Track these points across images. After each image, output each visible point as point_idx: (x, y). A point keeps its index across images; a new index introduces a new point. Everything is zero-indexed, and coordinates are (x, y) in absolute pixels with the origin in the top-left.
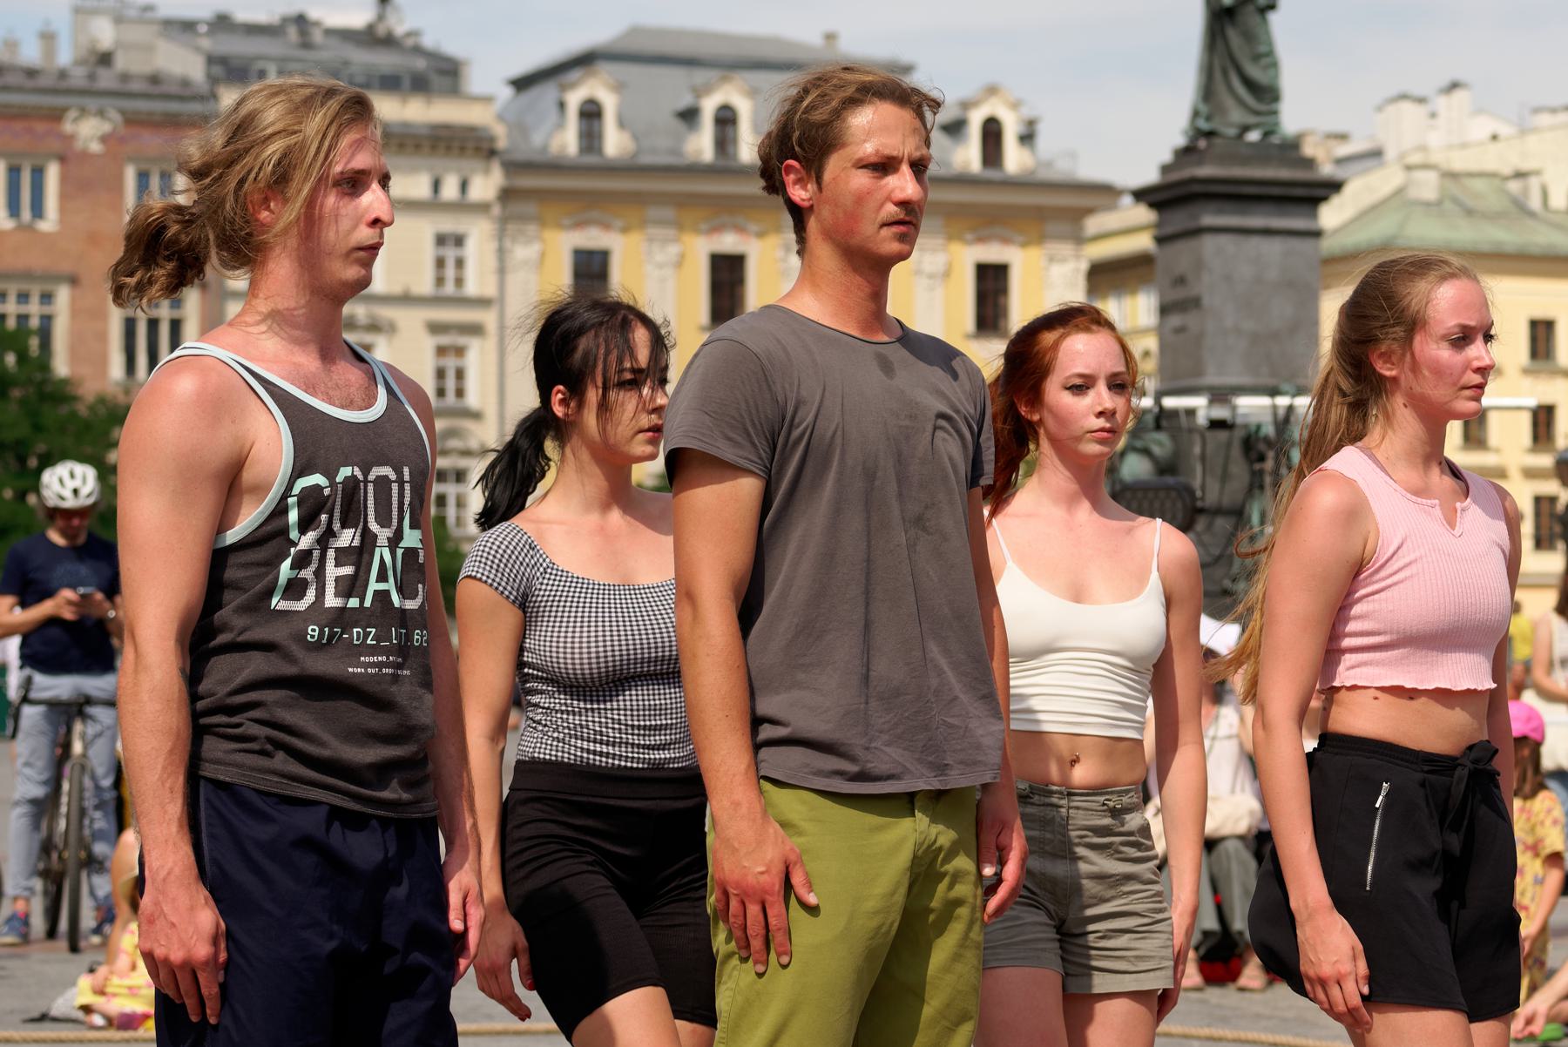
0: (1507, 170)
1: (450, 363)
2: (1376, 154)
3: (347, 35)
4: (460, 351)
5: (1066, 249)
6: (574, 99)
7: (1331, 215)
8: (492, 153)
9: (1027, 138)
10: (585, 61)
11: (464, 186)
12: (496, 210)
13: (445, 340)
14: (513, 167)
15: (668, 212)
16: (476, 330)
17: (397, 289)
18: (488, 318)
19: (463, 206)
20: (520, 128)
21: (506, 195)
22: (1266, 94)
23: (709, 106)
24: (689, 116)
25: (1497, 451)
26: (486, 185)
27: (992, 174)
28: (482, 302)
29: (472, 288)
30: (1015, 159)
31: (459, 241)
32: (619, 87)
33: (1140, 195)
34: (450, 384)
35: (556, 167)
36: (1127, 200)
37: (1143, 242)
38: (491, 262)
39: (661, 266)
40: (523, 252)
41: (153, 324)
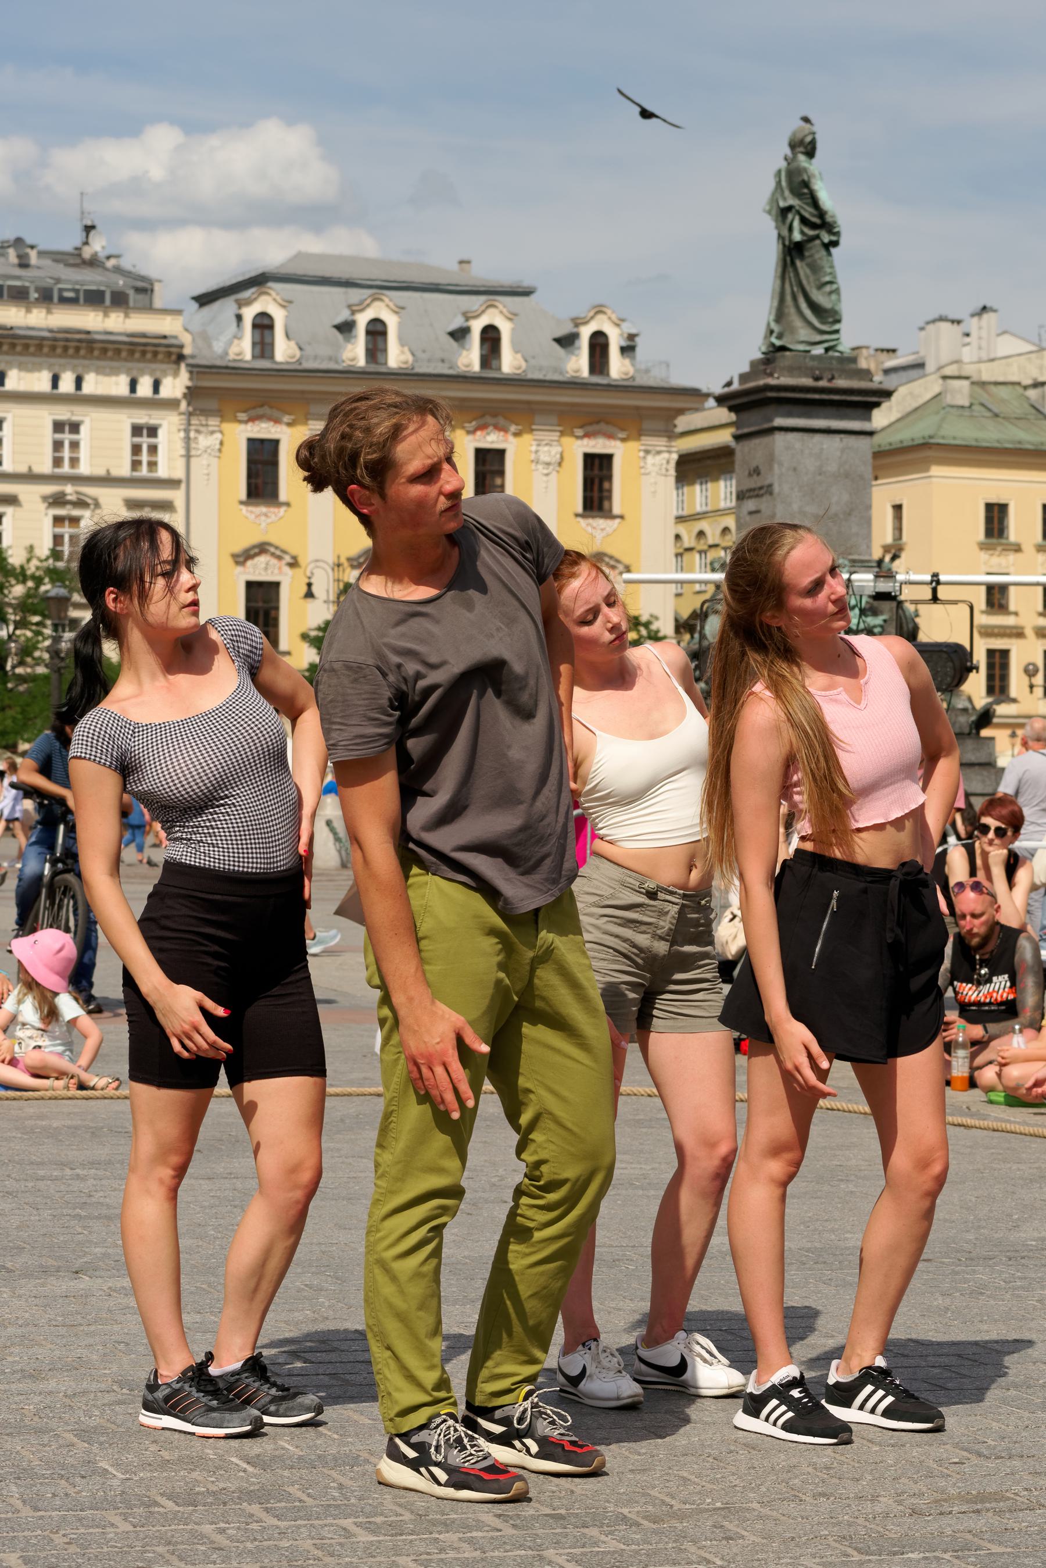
0: (1028, 382)
2: (921, 365)
3: (58, 257)
5: (660, 442)
6: (249, 313)
7: (880, 418)
8: (181, 357)
9: (627, 350)
10: (259, 281)
11: (156, 386)
12: (184, 405)
14: (198, 370)
17: (101, 472)
18: (177, 496)
19: (155, 403)
20: (203, 337)
21: (191, 393)
22: (828, 316)
23: (362, 320)
24: (346, 328)
25: (1016, 614)
26: (174, 386)
27: (597, 379)
28: (172, 483)
29: (162, 472)
30: (618, 367)
31: (153, 431)
32: (286, 304)
33: (721, 400)
35: (234, 370)
36: (711, 402)
37: (724, 437)
40: (205, 441)
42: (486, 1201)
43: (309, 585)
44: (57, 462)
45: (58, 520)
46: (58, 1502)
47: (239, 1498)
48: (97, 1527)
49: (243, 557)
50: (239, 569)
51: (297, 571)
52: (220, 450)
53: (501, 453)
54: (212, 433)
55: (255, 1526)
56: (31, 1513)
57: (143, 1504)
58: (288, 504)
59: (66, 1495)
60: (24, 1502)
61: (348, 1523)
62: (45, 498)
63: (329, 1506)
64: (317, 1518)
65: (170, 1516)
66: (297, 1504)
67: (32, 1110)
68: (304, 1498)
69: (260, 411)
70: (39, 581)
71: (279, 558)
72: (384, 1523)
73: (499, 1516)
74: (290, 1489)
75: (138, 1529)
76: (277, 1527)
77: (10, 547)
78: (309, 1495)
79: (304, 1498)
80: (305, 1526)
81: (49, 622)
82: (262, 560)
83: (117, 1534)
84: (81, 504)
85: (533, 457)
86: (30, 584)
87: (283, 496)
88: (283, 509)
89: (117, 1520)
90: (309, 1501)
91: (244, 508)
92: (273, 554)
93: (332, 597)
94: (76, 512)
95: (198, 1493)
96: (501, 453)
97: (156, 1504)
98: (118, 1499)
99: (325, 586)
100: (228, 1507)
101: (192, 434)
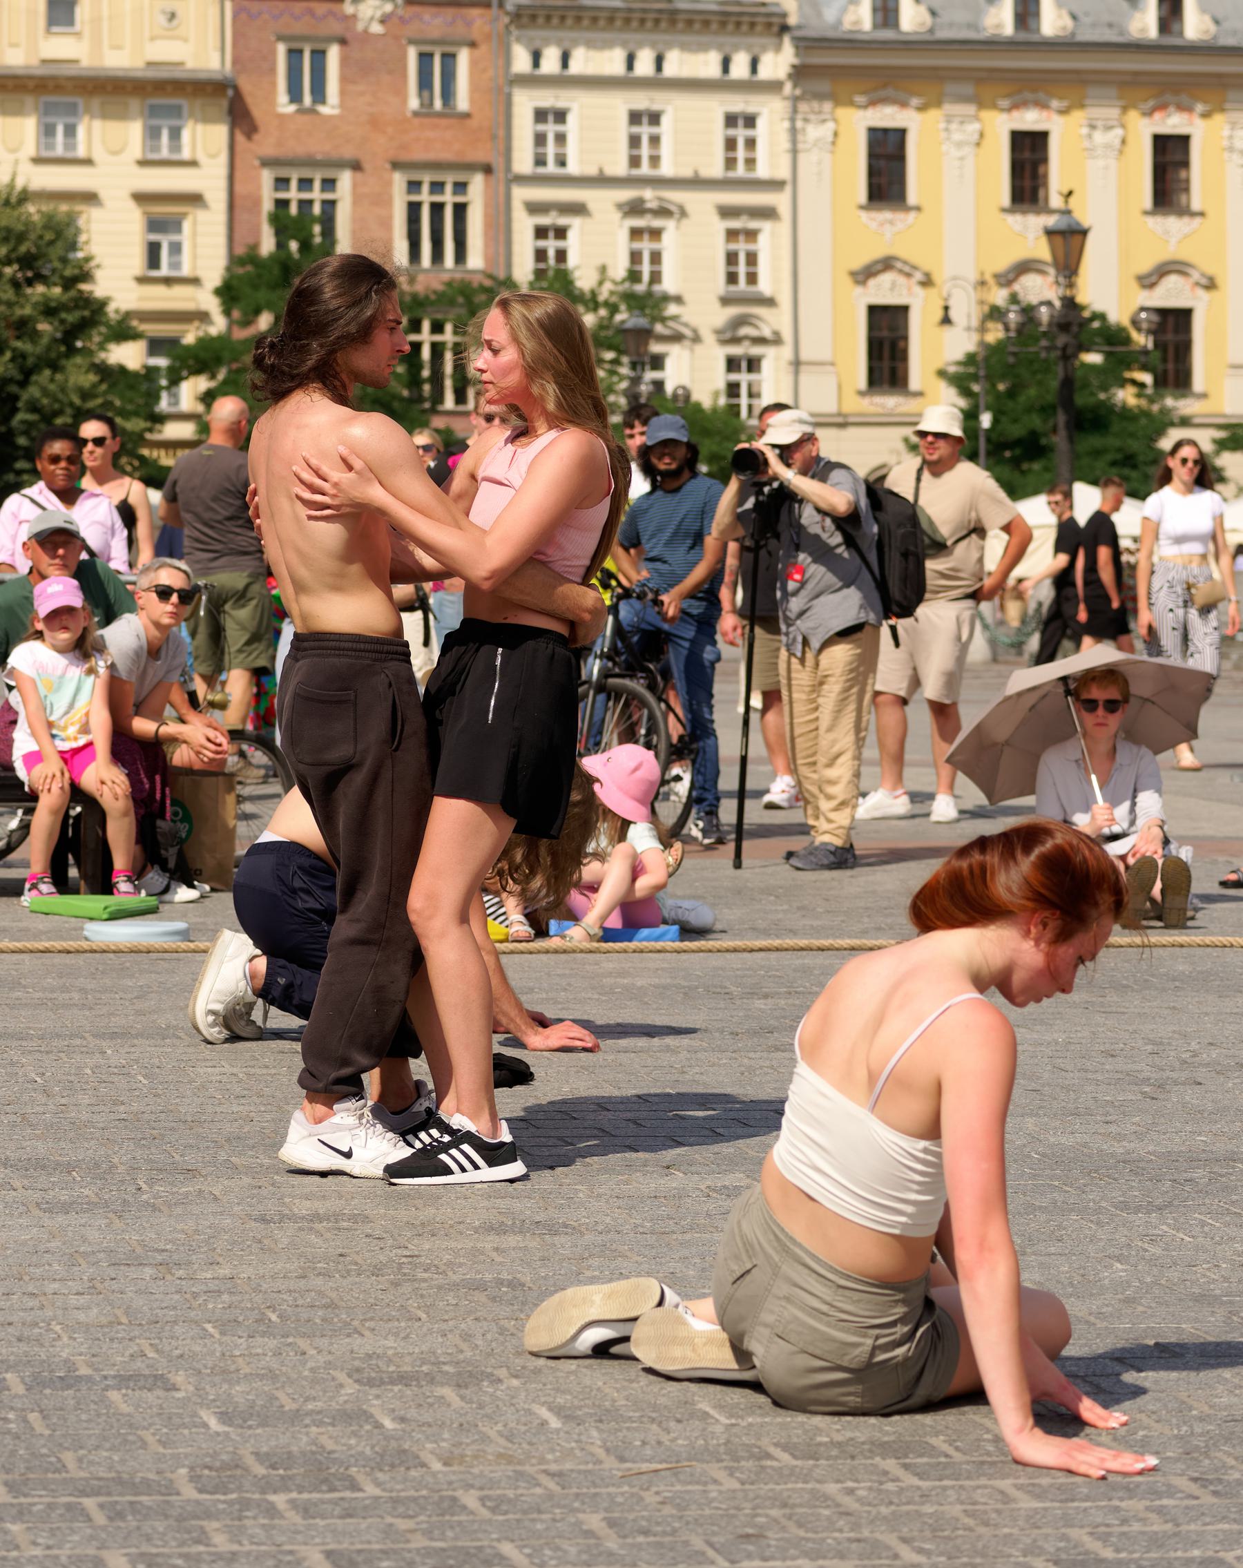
1: (741, 247)
4: (752, 235)
8: (784, 28)
13: (735, 224)
15: (969, 89)
16: (768, 213)
17: (687, 173)
19: (753, 86)
21: (799, 73)
26: (778, 62)
28: (775, 185)
29: (763, 171)
31: (750, 121)
34: (742, 269)
35: (851, 43)
38: (784, 142)
39: (959, 145)
40: (816, 132)
41: (437, 208)
42: (1176, 1083)
43: (946, 308)
44: (635, 161)
45: (636, 233)
46: (648, 1451)
47: (871, 1451)
48: (698, 1483)
49: (864, 275)
50: (859, 290)
51: (932, 292)
52: (833, 143)
53: (1184, 140)
54: (824, 121)
55: (890, 1486)
56: (616, 1464)
57: (752, 1456)
58: (918, 209)
59: (659, 1443)
60: (608, 1451)
61: (1006, 1484)
62: (620, 206)
63: (983, 1463)
64: (968, 1478)
65: (786, 1472)
66: (943, 1459)
67: (611, 965)
68: (951, 1451)
69: (882, 93)
70: (614, 309)
71: (908, 275)
72: (1052, 1485)
73: (1195, 1480)
74: (934, 1441)
75: (747, 1487)
76: (919, 1488)
77: (577, 267)
78: (957, 1449)
79: (951, 1451)
80: (953, 1487)
81: (625, 360)
82: (886, 278)
83: (720, 1492)
84: (663, 212)
85: (1225, 143)
86: (603, 312)
87: (912, 197)
88: (912, 215)
89: (721, 1475)
90: (958, 1456)
91: (864, 215)
92: (901, 271)
93: (975, 323)
94: (656, 223)
95: (820, 1444)
96: (1184, 140)
97: (769, 1456)
98: (722, 1449)
99: (966, 310)
100: (856, 1462)
101: (799, 124)
